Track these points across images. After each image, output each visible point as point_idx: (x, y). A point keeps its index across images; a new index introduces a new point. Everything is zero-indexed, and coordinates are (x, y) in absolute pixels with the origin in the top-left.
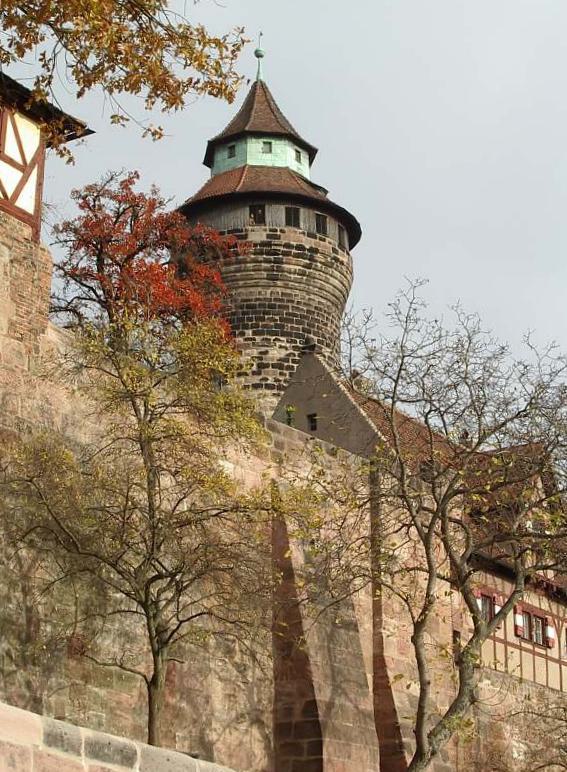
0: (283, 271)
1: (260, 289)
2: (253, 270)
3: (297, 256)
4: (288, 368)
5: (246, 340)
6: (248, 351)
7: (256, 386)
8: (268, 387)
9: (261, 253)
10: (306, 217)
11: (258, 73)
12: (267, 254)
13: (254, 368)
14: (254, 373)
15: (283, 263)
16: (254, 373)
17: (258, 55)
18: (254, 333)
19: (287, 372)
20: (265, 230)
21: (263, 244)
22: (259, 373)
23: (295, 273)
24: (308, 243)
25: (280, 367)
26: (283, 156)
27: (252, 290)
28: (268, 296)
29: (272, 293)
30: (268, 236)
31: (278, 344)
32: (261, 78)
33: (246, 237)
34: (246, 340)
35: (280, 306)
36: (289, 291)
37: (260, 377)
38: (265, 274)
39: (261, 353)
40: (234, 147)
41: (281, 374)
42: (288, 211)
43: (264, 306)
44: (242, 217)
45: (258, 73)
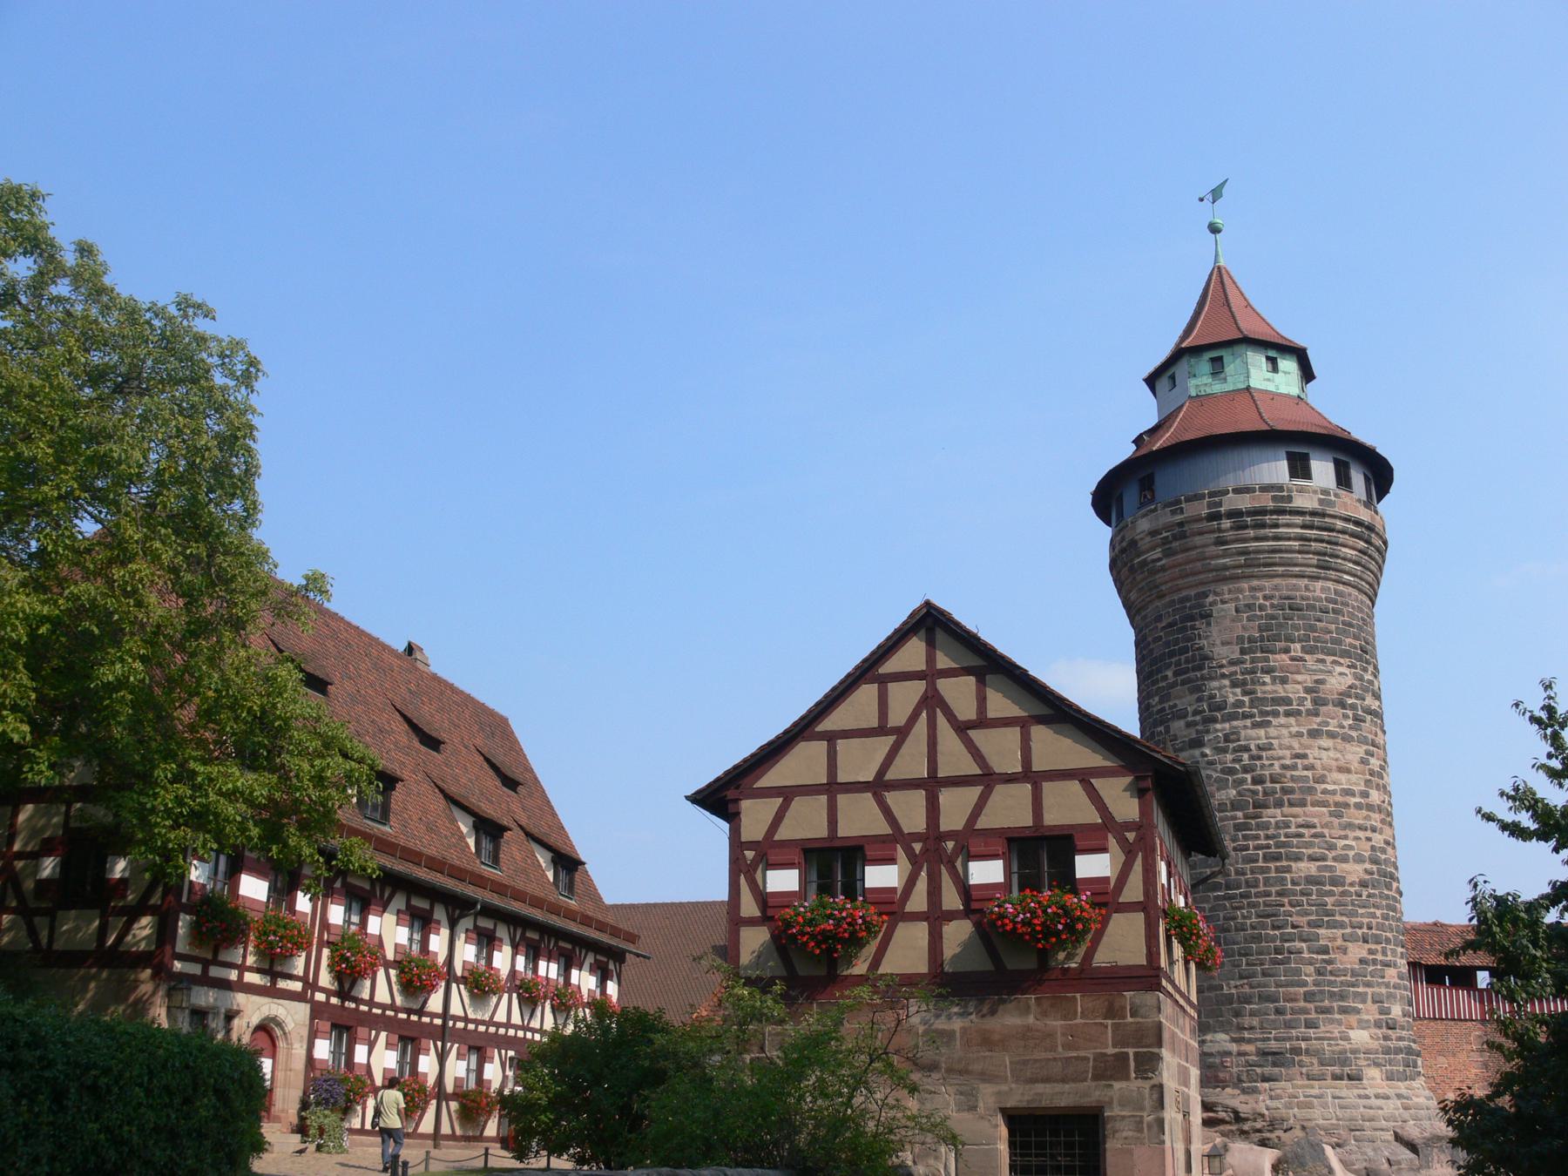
0: (1337, 557)
1: (1306, 581)
2: (1299, 552)
3: (1353, 535)
4: (1353, 707)
5: (1292, 659)
6: (1299, 678)
7: (1314, 734)
8: (1332, 735)
9: (1311, 527)
10: (1323, 470)
11: (1217, 255)
12: (1319, 528)
13: (1308, 705)
14: (1310, 713)
15: (1336, 544)
16: (1310, 713)
17: (1214, 229)
18: (1304, 650)
19: (1350, 713)
20: (1315, 492)
21: (1313, 513)
22: (1317, 715)
23: (1350, 561)
24: (1364, 515)
25: (1343, 705)
26: (1286, 379)
27: (1294, 581)
28: (1318, 593)
29: (1323, 589)
30: (1321, 501)
31: (1339, 669)
32: (1222, 263)
33: (1290, 499)
34: (1292, 659)
35: (1335, 611)
36: (1341, 587)
37: (1318, 720)
38: (1314, 559)
39: (1317, 681)
40: (1220, 359)
41: (1346, 717)
42: (1337, 463)
43: (1313, 608)
44: (1275, 469)
45: (1217, 255)
